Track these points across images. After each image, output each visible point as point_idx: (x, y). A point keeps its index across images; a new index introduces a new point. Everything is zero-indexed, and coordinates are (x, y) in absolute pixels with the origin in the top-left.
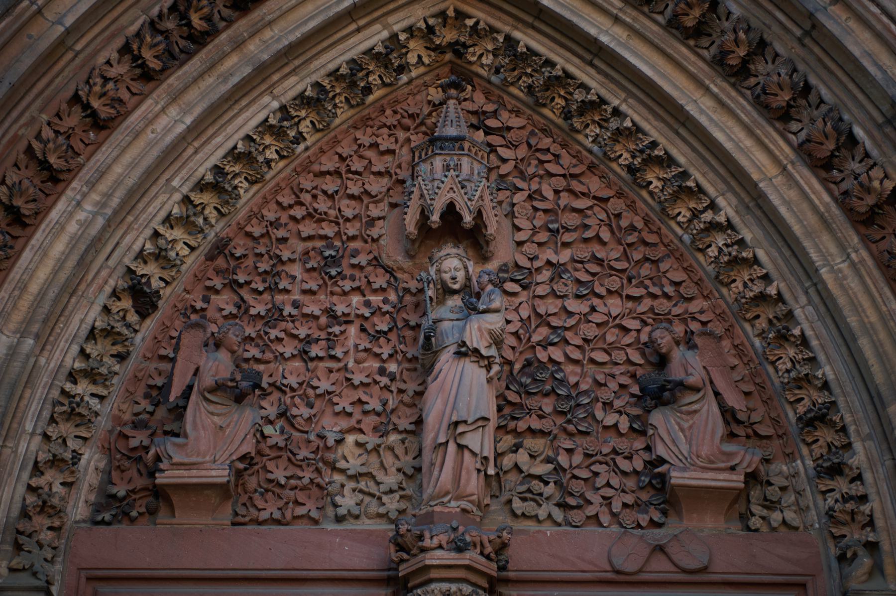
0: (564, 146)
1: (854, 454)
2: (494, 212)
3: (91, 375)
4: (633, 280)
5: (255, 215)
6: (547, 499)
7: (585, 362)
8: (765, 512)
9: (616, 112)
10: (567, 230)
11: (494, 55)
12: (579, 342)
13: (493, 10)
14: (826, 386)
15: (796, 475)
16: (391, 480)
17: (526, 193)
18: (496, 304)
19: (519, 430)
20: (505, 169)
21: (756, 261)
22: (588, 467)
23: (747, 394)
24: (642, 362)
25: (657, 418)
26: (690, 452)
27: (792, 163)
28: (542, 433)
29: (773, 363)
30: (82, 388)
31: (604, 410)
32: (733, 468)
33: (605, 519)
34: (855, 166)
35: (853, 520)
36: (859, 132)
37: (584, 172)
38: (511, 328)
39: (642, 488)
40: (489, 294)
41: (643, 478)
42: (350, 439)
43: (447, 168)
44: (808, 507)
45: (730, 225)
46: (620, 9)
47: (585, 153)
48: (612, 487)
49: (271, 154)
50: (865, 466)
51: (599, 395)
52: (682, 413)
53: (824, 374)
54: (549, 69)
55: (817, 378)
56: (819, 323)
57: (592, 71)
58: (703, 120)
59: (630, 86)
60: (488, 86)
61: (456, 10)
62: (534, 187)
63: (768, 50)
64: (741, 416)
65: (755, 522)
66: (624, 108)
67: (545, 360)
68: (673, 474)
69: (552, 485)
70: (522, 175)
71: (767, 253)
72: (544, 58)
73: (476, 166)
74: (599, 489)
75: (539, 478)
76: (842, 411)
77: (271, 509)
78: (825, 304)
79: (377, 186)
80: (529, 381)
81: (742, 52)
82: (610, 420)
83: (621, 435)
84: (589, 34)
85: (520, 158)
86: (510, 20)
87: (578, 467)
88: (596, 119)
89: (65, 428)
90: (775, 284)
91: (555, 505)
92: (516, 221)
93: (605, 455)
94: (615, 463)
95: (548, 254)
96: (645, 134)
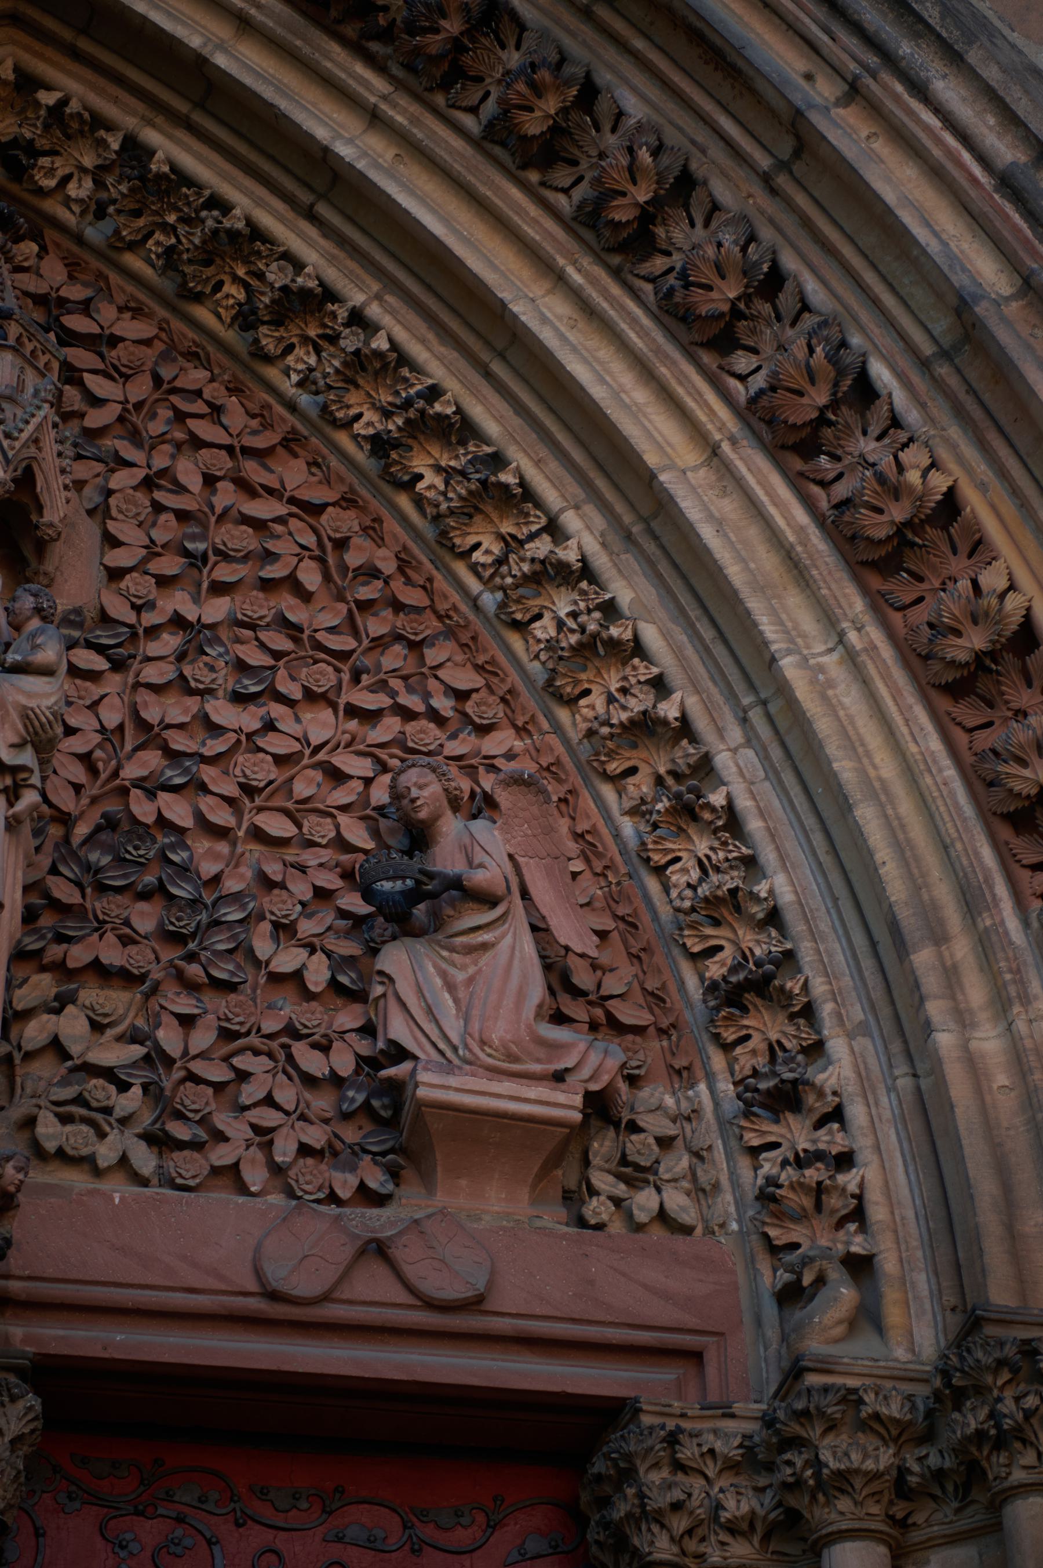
0: (235, 389)
1: (830, 1063)
2: (64, 494)
4: (364, 677)
6: (124, 1121)
7: (241, 834)
8: (621, 1189)
9: (357, 318)
10: (224, 555)
11: (94, 181)
12: (230, 789)
13: (102, 82)
14: (774, 918)
15: (693, 1115)
17: (140, 474)
18: (49, 653)
19: (71, 964)
20: (96, 419)
21: (638, 649)
22: (226, 1059)
23: (602, 935)
24: (370, 845)
26: (466, 1032)
27: (733, 441)
28: (127, 978)
29: (659, 871)
31: (277, 940)
32: (559, 1077)
33: (255, 1176)
34: (868, 446)
35: (818, 1206)
36: (880, 372)
37: (274, 447)
39: (347, 1117)
40: (33, 636)
41: (351, 1094)
44: (716, 1186)
45: (586, 572)
46: (384, 98)
47: (279, 409)
48: (278, 1107)
50: (851, 1088)
51: (267, 906)
52: (452, 950)
53: (771, 892)
54: (216, 213)
55: (755, 898)
56: (767, 784)
57: (312, 231)
58: (547, 336)
59: (391, 266)
60: (75, 249)
61: (17, 69)
62: (160, 462)
63: (698, 196)
64: (583, 978)
65: (597, 1209)
66: (374, 311)
67: (150, 820)
68: (423, 1076)
69: (136, 1091)
70: (135, 437)
71: (665, 635)
72: (207, 193)
73: (31, 379)
74: (247, 1108)
75: (108, 1074)
76: (808, 971)
78: (783, 744)
80: (106, 860)
81: (642, 195)
82: (287, 961)
83: (309, 996)
84: (311, 137)
85: (133, 399)
86: (140, 107)
87: (200, 1056)
88: (312, 333)
90: (677, 696)
91: (140, 1136)
92: (111, 526)
93: (270, 1037)
94: (290, 1058)
95: (180, 602)
96: (416, 368)
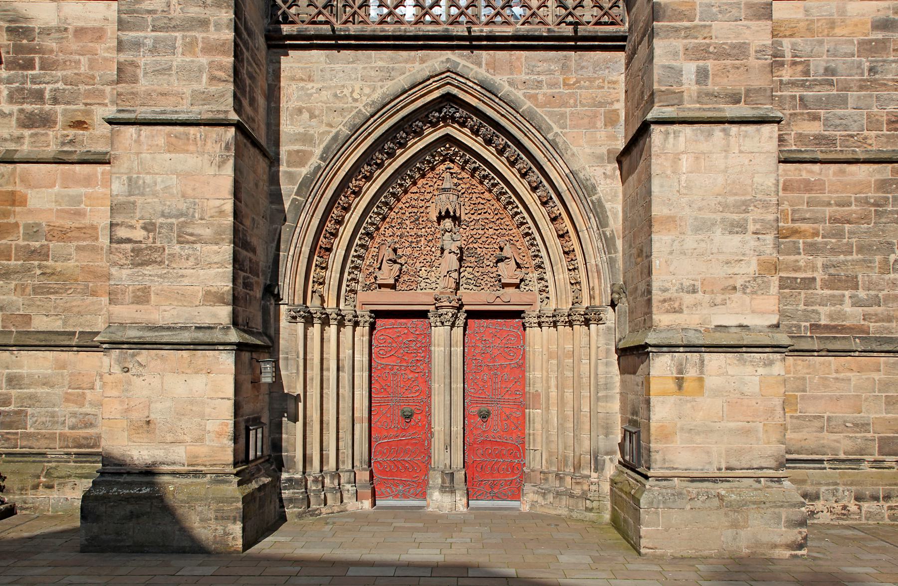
16: (434, 279)
17: (468, 199)
21: (527, 223)
25: (499, 264)
28: (470, 267)
33: (486, 289)
38: (464, 238)
42: (423, 269)
45: (521, 212)
65: (522, 289)
77: (404, 287)
79: (428, 197)
95: (473, 217)
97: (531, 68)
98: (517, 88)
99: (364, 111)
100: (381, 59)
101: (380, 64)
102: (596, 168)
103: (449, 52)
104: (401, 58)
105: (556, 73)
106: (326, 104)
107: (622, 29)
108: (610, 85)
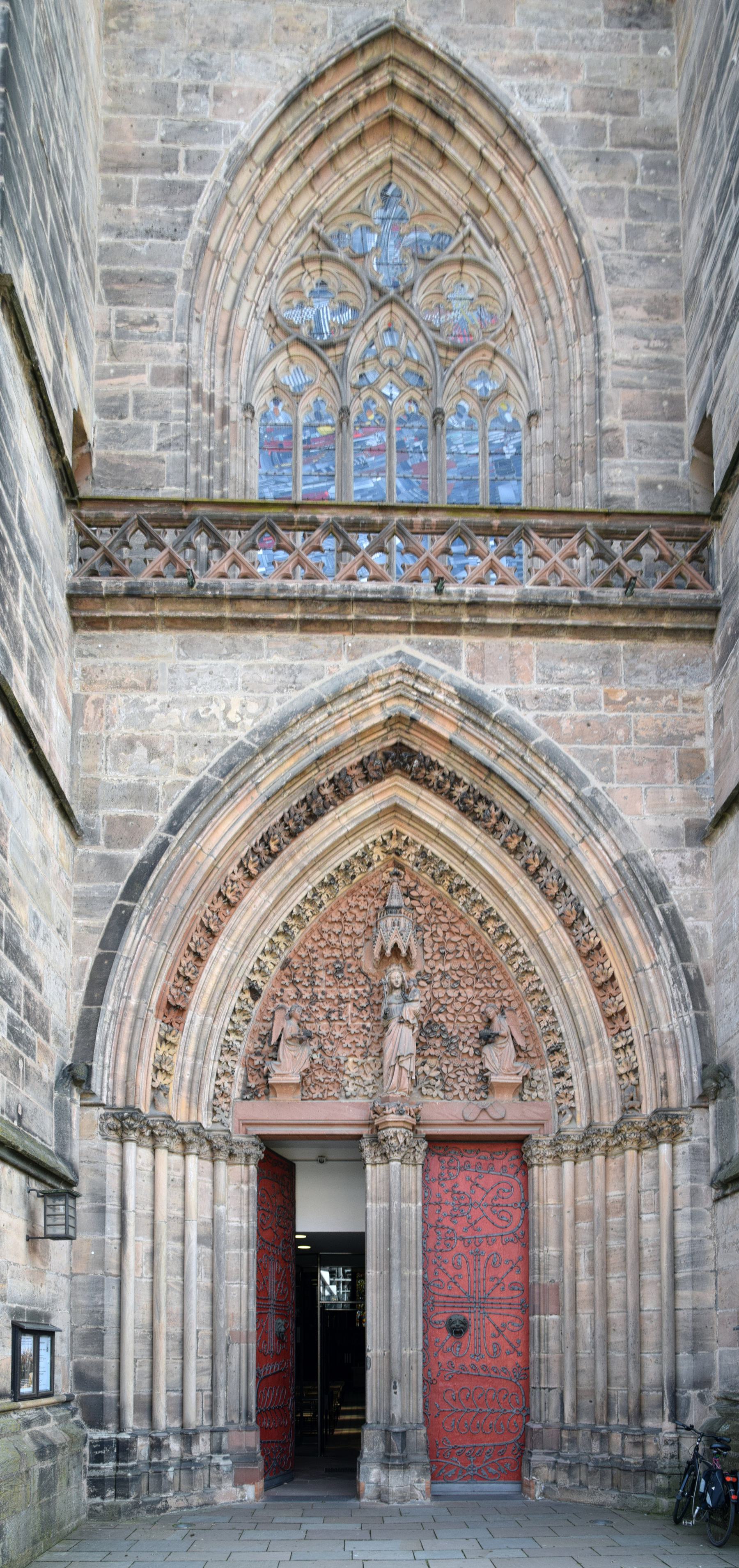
3: (235, 1031)
5: (302, 946)
9: (474, 890)
30: (232, 1037)
43: (394, 924)
49: (308, 914)
89: (227, 1057)
97: (548, 671)
98: (524, 707)
99: (248, 742)
100: (279, 651)
101: (276, 659)
102: (666, 855)
103: (402, 638)
104: (315, 651)
105: (593, 682)
106: (179, 730)
107: (711, 595)
108: (686, 706)
